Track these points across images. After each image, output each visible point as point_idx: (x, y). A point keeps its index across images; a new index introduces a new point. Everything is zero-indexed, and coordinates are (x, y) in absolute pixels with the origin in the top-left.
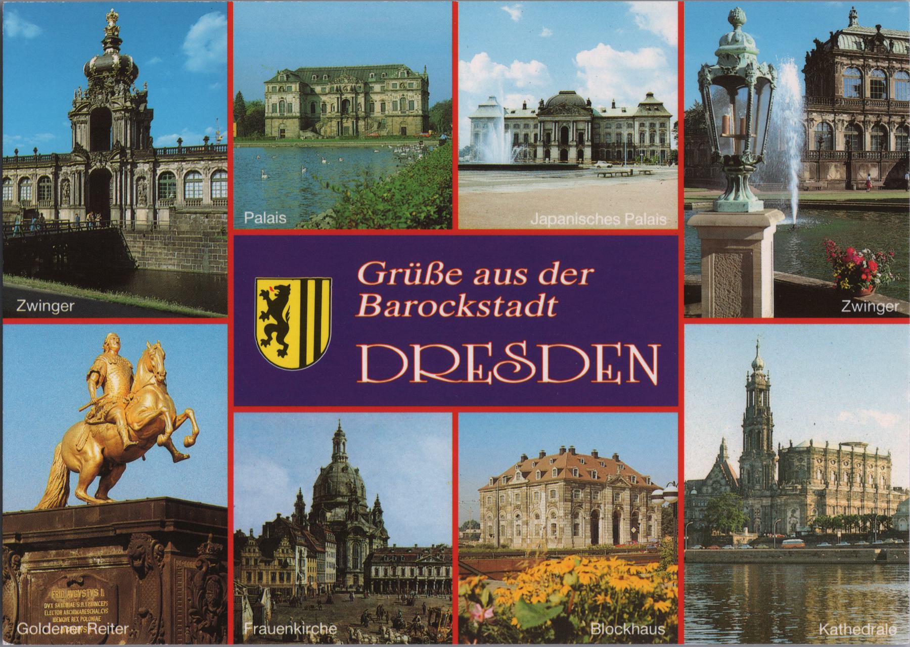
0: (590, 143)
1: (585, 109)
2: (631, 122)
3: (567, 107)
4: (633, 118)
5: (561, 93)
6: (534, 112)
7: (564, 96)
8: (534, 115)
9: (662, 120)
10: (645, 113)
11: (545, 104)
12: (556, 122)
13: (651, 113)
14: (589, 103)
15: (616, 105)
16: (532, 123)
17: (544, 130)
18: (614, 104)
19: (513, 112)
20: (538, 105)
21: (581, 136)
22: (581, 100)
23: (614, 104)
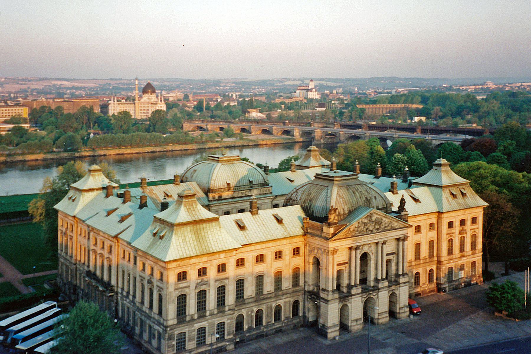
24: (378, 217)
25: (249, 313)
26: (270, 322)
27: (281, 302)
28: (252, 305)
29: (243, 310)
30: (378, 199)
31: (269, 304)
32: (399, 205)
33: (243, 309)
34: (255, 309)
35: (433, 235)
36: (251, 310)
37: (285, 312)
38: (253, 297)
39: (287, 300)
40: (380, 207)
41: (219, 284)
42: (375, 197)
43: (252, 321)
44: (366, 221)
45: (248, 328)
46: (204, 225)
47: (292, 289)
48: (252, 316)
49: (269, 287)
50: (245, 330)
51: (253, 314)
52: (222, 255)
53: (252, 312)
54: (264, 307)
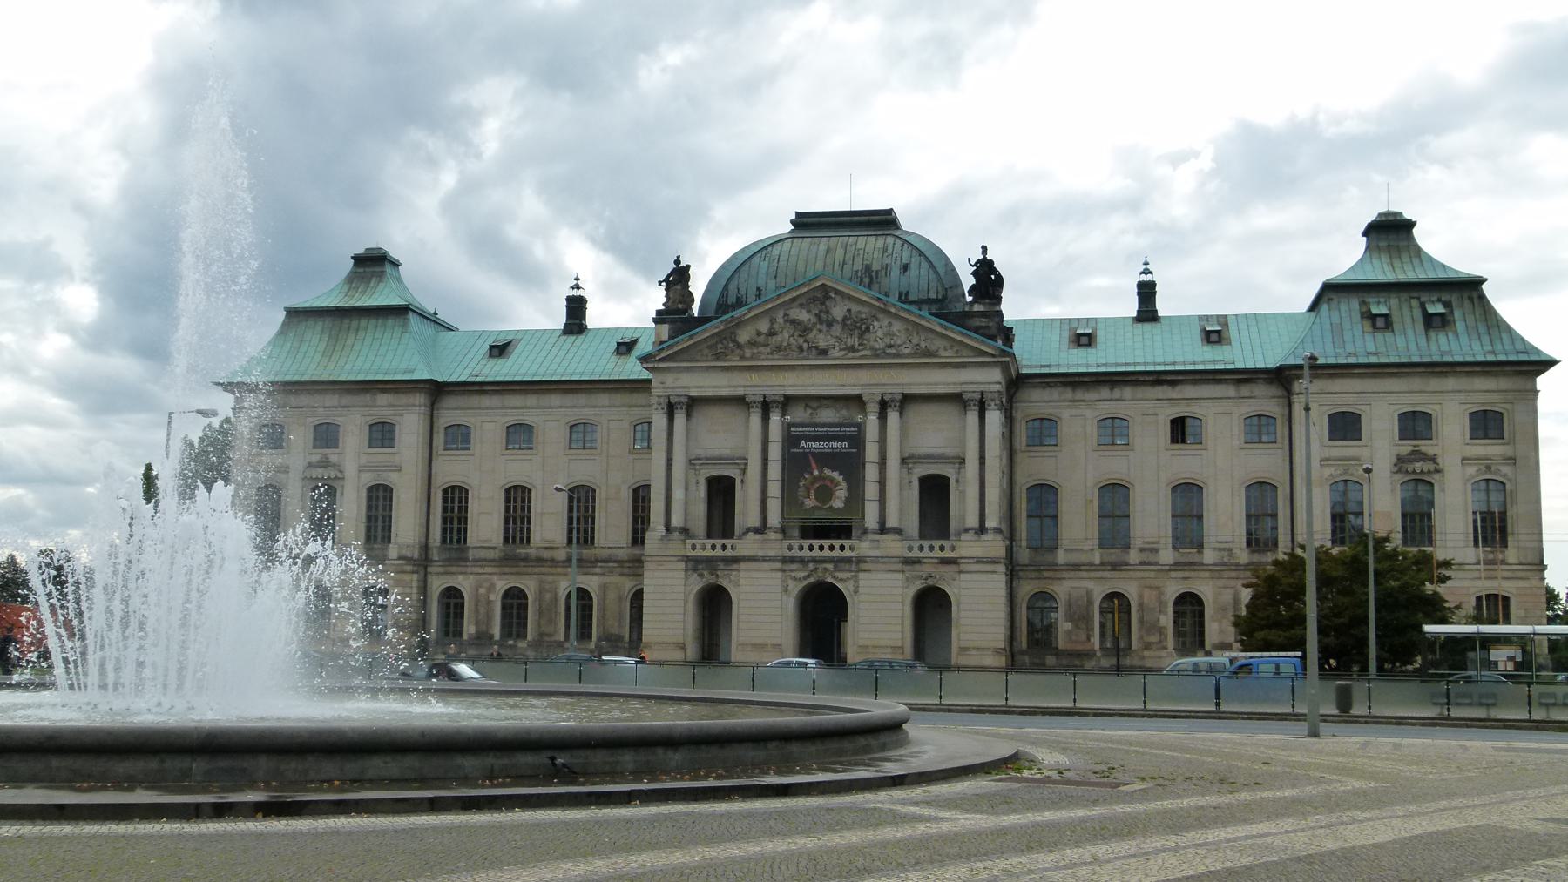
0: (994, 546)
1: (961, 319)
2: (1264, 400)
3: (838, 312)
4: (1282, 377)
5: (806, 223)
6: (625, 347)
7: (818, 245)
8: (632, 368)
9: (1486, 393)
10: (1363, 346)
11: (698, 286)
12: (766, 407)
13: (1408, 343)
14: (988, 279)
15: (1163, 307)
16: (612, 418)
17: (691, 462)
18: (1147, 292)
19: (500, 350)
20: (657, 298)
21: (935, 492)
22: (932, 259)
23: (1147, 292)
24: (855, 308)
25: (482, 591)
26: (550, 635)
27: (592, 583)
28: (489, 570)
29: (460, 577)
30: (913, 271)
31: (550, 578)
32: (973, 281)
33: (461, 573)
34: (502, 585)
35: (1265, 463)
36: (486, 585)
37: (603, 618)
38: (494, 548)
39: (607, 579)
40: (912, 297)
41: (369, 479)
42: (905, 268)
43: (489, 617)
44: (803, 316)
45: (477, 632)
46: (363, 323)
47: (629, 551)
48: (489, 602)
49: (549, 525)
50: (465, 637)
51: (492, 597)
52: (383, 399)
53: (491, 588)
54: (529, 585)
